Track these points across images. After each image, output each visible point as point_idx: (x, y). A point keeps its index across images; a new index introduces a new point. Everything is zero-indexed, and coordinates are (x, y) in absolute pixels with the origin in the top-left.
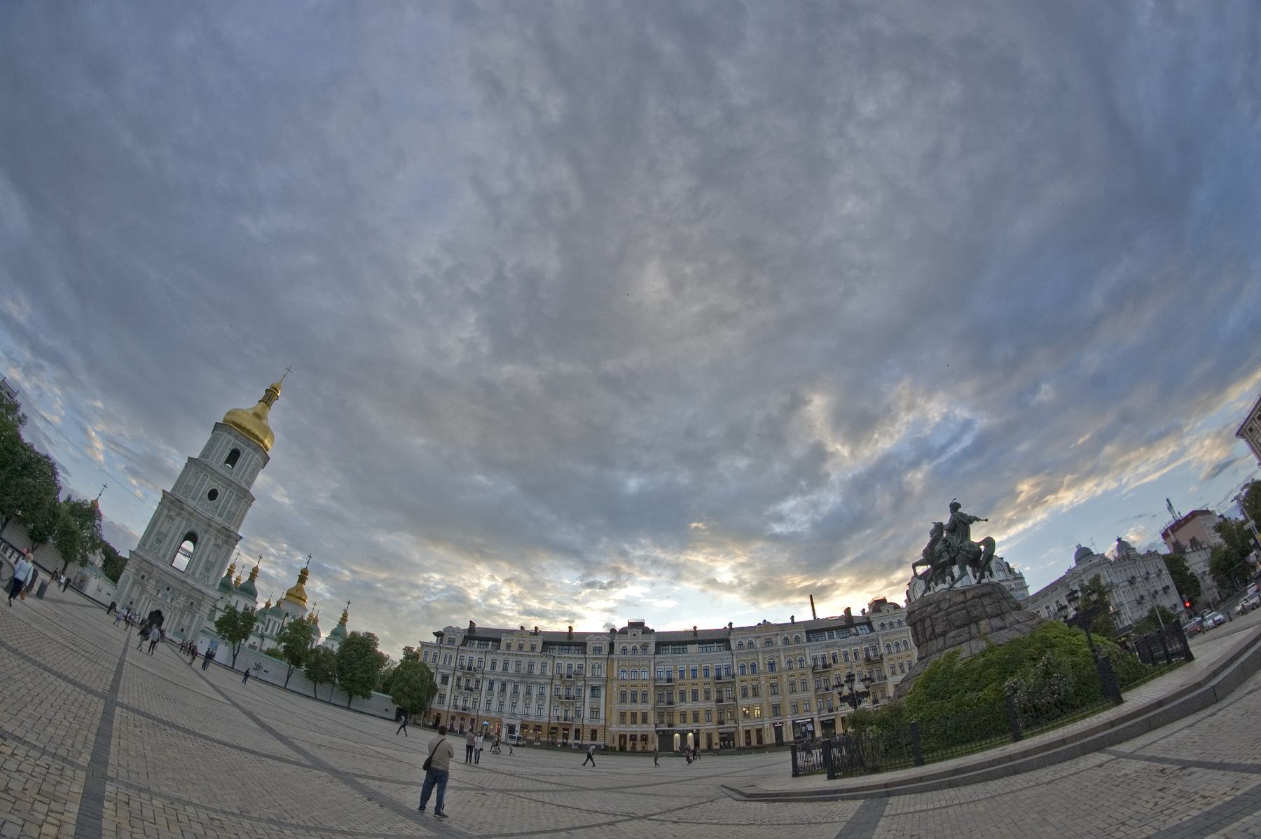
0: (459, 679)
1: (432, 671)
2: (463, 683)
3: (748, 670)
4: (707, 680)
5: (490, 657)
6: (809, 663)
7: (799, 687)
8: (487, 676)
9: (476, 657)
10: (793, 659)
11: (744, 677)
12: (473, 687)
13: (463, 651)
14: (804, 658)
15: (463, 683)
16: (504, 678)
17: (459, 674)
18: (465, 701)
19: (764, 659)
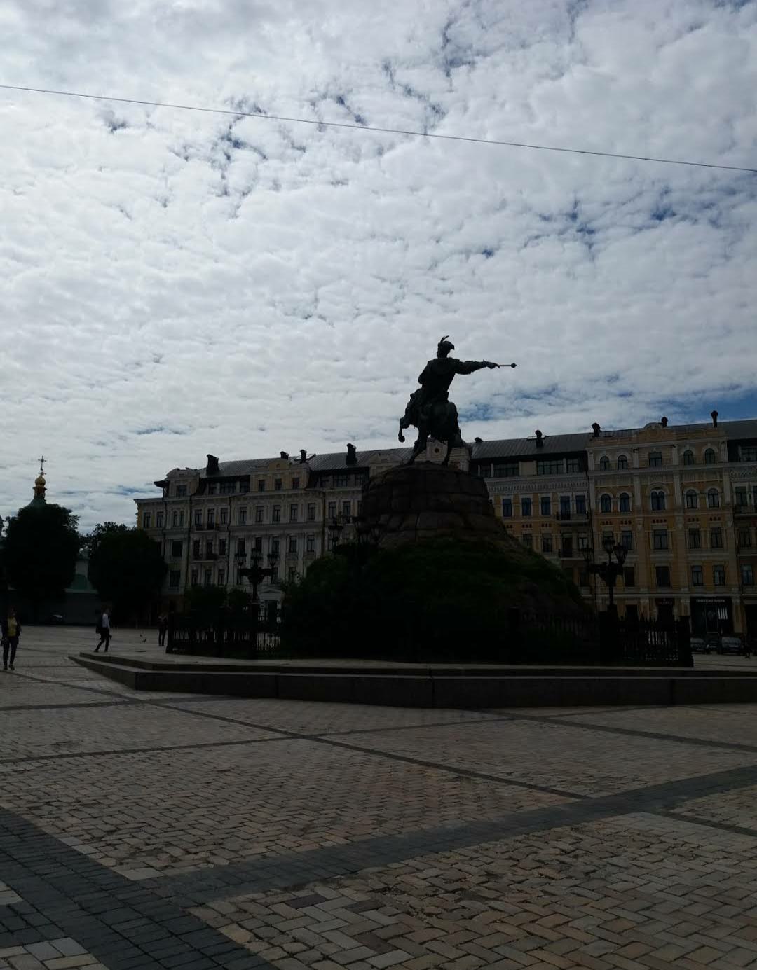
0: (197, 543)
1: (158, 539)
2: (203, 550)
3: (615, 506)
4: (546, 520)
5: (236, 505)
6: (728, 499)
7: (706, 540)
8: (236, 534)
9: (218, 509)
10: (698, 492)
11: (608, 517)
12: (218, 552)
13: (198, 502)
14: (719, 490)
15: (203, 550)
16: (258, 534)
17: (195, 537)
18: (208, 575)
19: (643, 488)
